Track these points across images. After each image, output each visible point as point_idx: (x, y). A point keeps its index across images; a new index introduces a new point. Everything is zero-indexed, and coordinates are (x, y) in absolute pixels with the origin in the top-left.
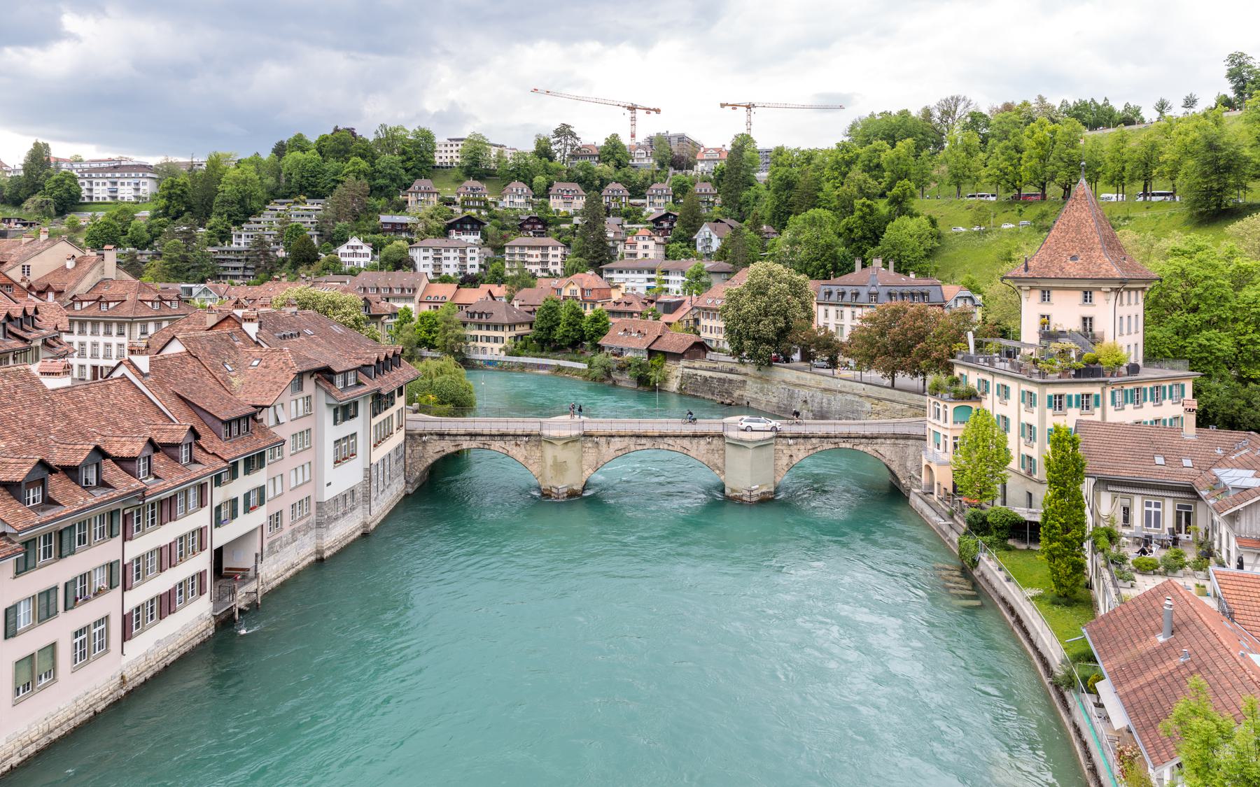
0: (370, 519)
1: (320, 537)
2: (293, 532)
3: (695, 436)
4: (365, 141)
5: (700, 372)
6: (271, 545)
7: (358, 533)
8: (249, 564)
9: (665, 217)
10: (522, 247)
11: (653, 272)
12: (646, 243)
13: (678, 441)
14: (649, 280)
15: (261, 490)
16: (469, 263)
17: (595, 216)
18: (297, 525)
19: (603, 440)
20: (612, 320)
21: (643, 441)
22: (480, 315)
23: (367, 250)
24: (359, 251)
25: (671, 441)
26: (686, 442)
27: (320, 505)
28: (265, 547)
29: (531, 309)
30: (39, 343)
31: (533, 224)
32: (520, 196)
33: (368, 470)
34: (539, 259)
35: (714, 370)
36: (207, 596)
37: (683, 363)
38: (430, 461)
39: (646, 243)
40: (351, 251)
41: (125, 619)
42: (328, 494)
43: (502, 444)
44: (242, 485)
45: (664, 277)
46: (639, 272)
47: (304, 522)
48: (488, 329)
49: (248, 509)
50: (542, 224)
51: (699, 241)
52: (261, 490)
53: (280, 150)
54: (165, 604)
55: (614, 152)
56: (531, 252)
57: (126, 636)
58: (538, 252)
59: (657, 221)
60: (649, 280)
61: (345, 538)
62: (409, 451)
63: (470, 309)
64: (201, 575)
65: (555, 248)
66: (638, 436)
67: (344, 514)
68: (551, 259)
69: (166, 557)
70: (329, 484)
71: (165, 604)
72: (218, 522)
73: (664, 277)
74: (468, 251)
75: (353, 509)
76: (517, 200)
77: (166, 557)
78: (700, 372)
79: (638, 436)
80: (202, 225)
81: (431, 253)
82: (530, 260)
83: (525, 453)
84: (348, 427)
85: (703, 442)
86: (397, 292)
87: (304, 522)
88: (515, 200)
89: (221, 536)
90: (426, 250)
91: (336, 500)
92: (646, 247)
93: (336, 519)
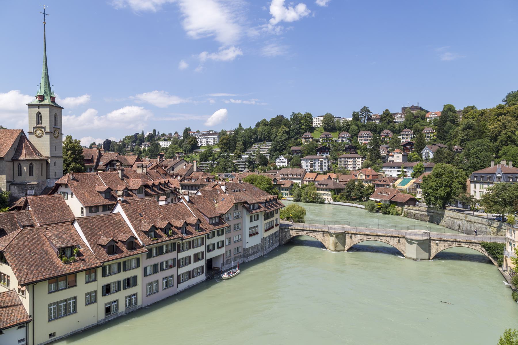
2: (235, 258)
3: (392, 237)
4: (287, 120)
5: (412, 211)
6: (227, 261)
8: (220, 266)
9: (409, 143)
10: (345, 158)
11: (400, 168)
12: (398, 155)
13: (385, 238)
14: (398, 171)
15: (223, 242)
16: (324, 164)
17: (376, 144)
18: (236, 255)
19: (353, 236)
21: (370, 237)
22: (324, 185)
23: (285, 160)
25: (381, 238)
26: (388, 239)
28: (225, 261)
29: (345, 183)
30: (170, 191)
31: (351, 149)
32: (345, 138)
34: (352, 163)
35: (418, 210)
36: (204, 275)
37: (405, 207)
38: (288, 238)
39: (398, 155)
41: (179, 277)
42: (247, 246)
43: (314, 234)
44: (216, 240)
45: (405, 170)
46: (394, 168)
47: (239, 254)
48: (285, 190)
49: (218, 247)
50: (353, 149)
51: (424, 154)
52: (223, 242)
53: (258, 125)
54: (191, 275)
55: (387, 117)
56: (348, 160)
57: (179, 282)
58: (352, 160)
59: (405, 146)
60: (398, 171)
63: (320, 183)
64: (203, 267)
65: (359, 158)
66: (367, 235)
68: (357, 163)
72: (209, 251)
73: (405, 170)
74: (323, 161)
76: (344, 139)
78: (412, 211)
79: (367, 235)
80: (232, 153)
81: (309, 162)
82: (348, 163)
83: (323, 238)
85: (396, 240)
86: (295, 176)
87: (239, 254)
88: (342, 139)
89: (209, 255)
90: (307, 160)
91: (250, 248)
92: (398, 157)
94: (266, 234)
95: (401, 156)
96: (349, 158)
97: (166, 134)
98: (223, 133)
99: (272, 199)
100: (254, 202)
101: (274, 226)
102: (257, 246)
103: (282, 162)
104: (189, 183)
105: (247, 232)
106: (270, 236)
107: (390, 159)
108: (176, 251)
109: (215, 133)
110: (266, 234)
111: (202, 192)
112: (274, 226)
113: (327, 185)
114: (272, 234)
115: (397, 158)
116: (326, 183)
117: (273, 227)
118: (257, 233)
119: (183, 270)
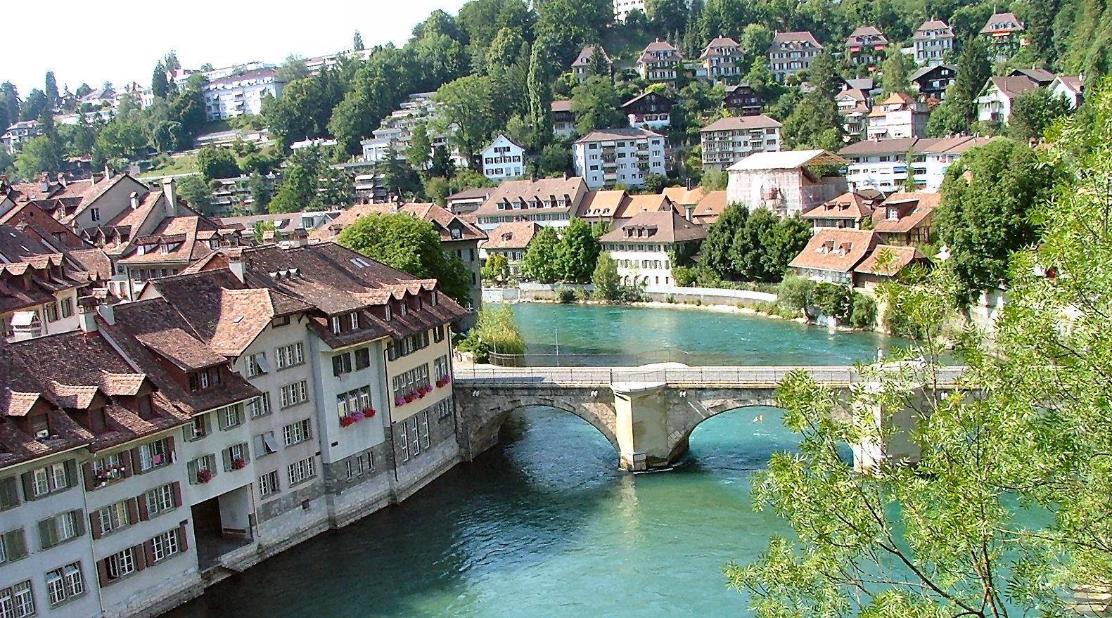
0: (396, 485)
1: (330, 503)
7: (384, 504)
8: (243, 524)
20: (816, 230)
24: (507, 154)
27: (326, 467)
33: (390, 432)
40: (498, 154)
42: (335, 455)
46: (883, 159)
53: (419, 32)
54: (143, 557)
58: (748, 138)
61: (366, 507)
62: (459, 409)
63: (629, 224)
64: (180, 531)
67: (361, 479)
69: (138, 510)
70: (335, 444)
71: (143, 557)
75: (373, 474)
77: (138, 510)
84: (354, 379)
91: (347, 462)
93: (350, 484)
94: (401, 414)
95: (906, 116)
96: (741, 132)
97: (98, 85)
98: (299, 69)
99: (415, 292)
100: (343, 308)
101: (433, 383)
102: (370, 454)
103: (504, 160)
104: (152, 258)
105: (333, 411)
106: (416, 416)
107: (873, 128)
108: (80, 487)
109: (267, 71)
110: (401, 414)
111: (159, 286)
112: (433, 383)
113: (653, 231)
114: (427, 411)
115: (895, 121)
116: (651, 224)
117: (428, 389)
118: (369, 413)
119: (110, 546)
